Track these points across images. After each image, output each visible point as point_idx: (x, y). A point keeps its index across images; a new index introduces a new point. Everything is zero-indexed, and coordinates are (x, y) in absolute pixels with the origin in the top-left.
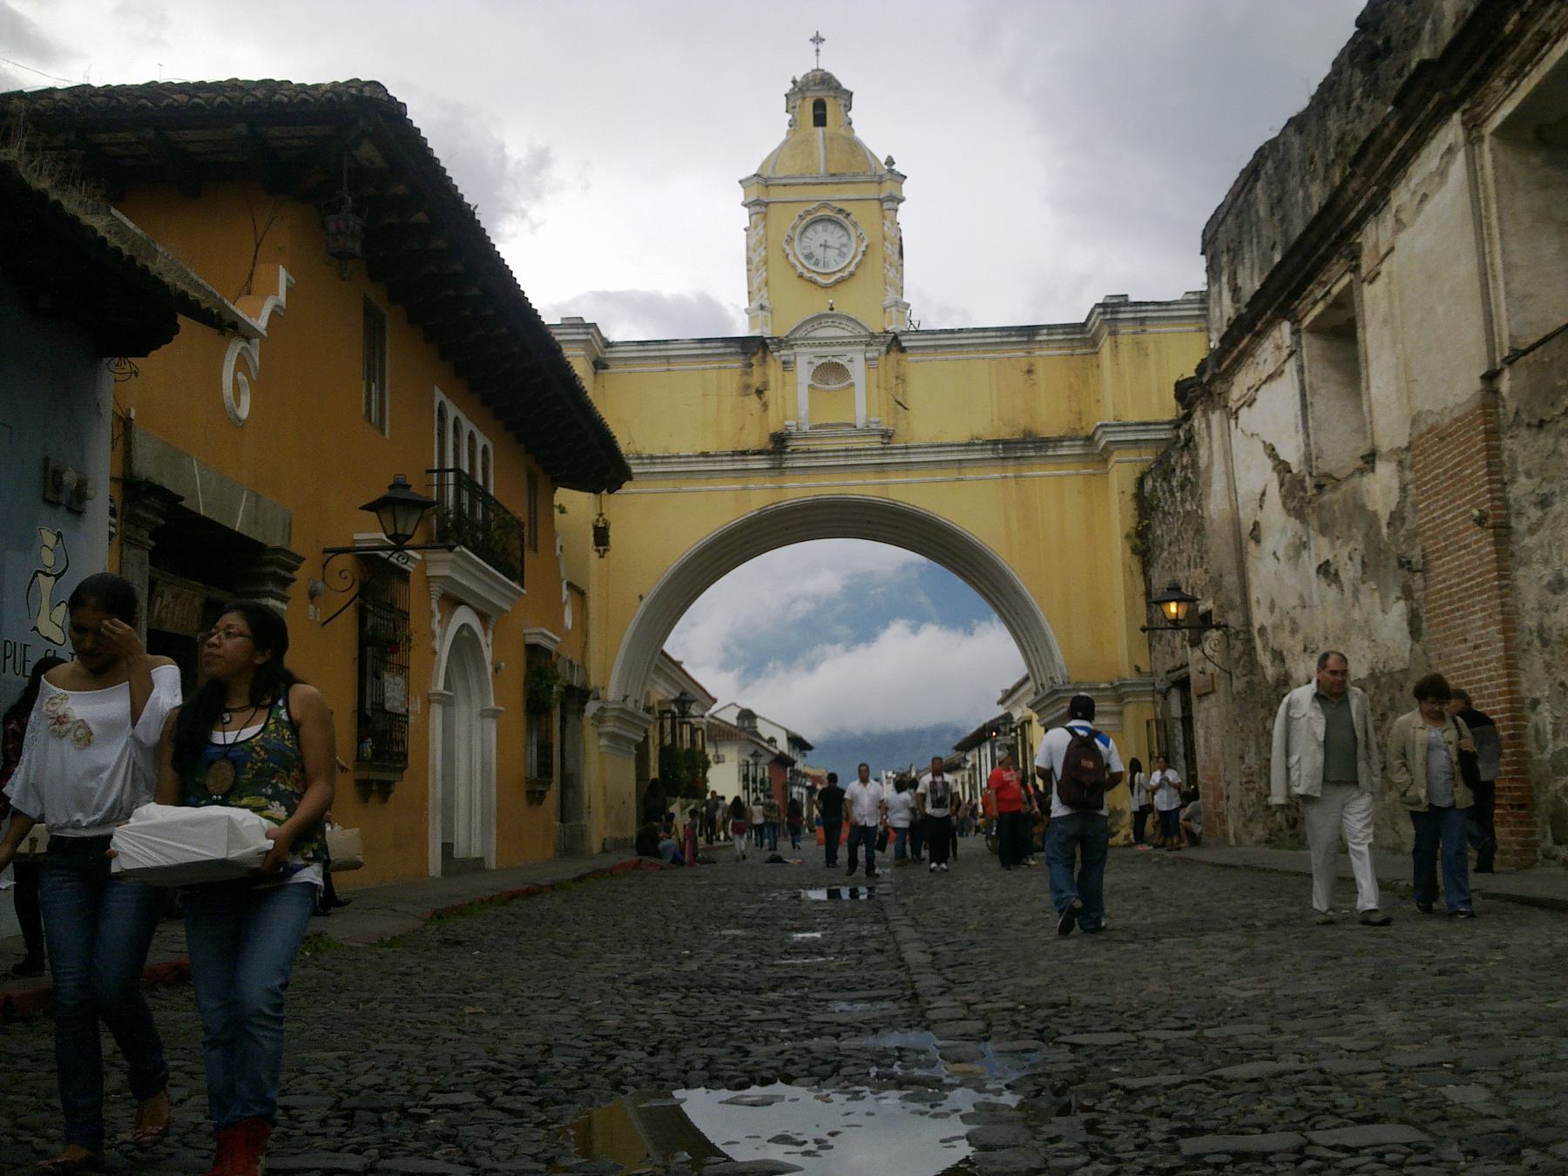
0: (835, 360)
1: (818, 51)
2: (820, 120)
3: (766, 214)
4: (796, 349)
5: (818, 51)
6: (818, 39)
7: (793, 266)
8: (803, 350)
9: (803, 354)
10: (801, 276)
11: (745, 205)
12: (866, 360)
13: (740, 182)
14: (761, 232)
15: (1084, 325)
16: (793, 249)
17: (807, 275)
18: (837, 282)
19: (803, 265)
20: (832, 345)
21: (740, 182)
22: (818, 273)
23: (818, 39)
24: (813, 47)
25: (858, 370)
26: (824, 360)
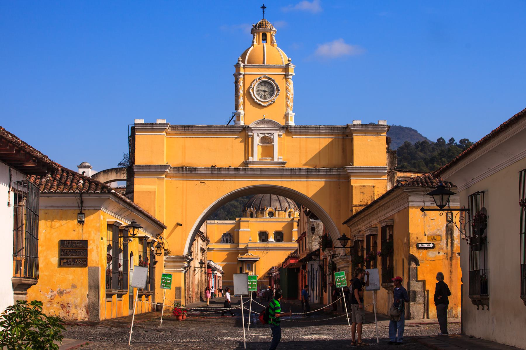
0: (267, 135)
1: (264, 12)
5: (264, 12)
6: (264, 7)
7: (253, 99)
10: (256, 102)
12: (279, 135)
13: (234, 65)
16: (253, 92)
17: (258, 102)
18: (269, 105)
19: (257, 99)
21: (234, 65)
22: (262, 102)
23: (264, 7)
24: (262, 10)
25: (276, 139)
26: (263, 135)
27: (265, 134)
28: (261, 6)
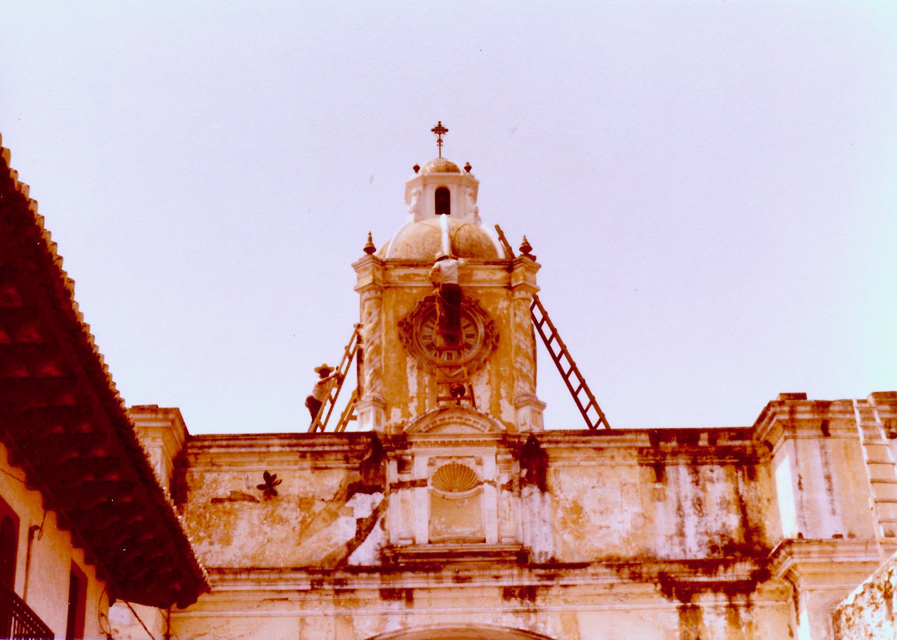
0: (459, 462)
1: (440, 141)
2: (443, 204)
3: (380, 299)
4: (414, 449)
5: (440, 141)
6: (440, 130)
8: (422, 449)
9: (424, 454)
11: (357, 290)
14: (376, 319)
15: (753, 430)
20: (457, 444)
23: (440, 130)
24: (436, 137)
26: (448, 462)
27: (454, 459)
28: (434, 128)
